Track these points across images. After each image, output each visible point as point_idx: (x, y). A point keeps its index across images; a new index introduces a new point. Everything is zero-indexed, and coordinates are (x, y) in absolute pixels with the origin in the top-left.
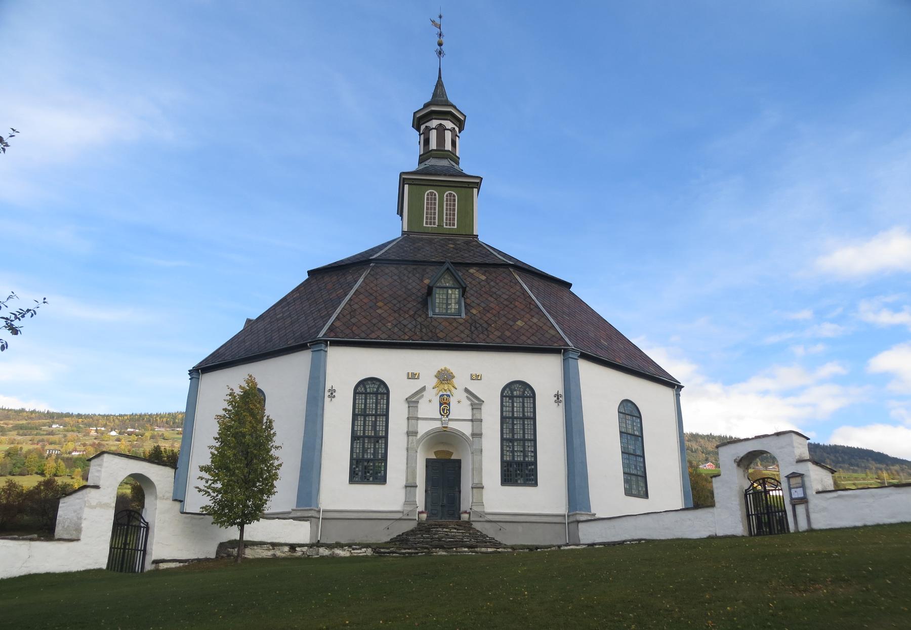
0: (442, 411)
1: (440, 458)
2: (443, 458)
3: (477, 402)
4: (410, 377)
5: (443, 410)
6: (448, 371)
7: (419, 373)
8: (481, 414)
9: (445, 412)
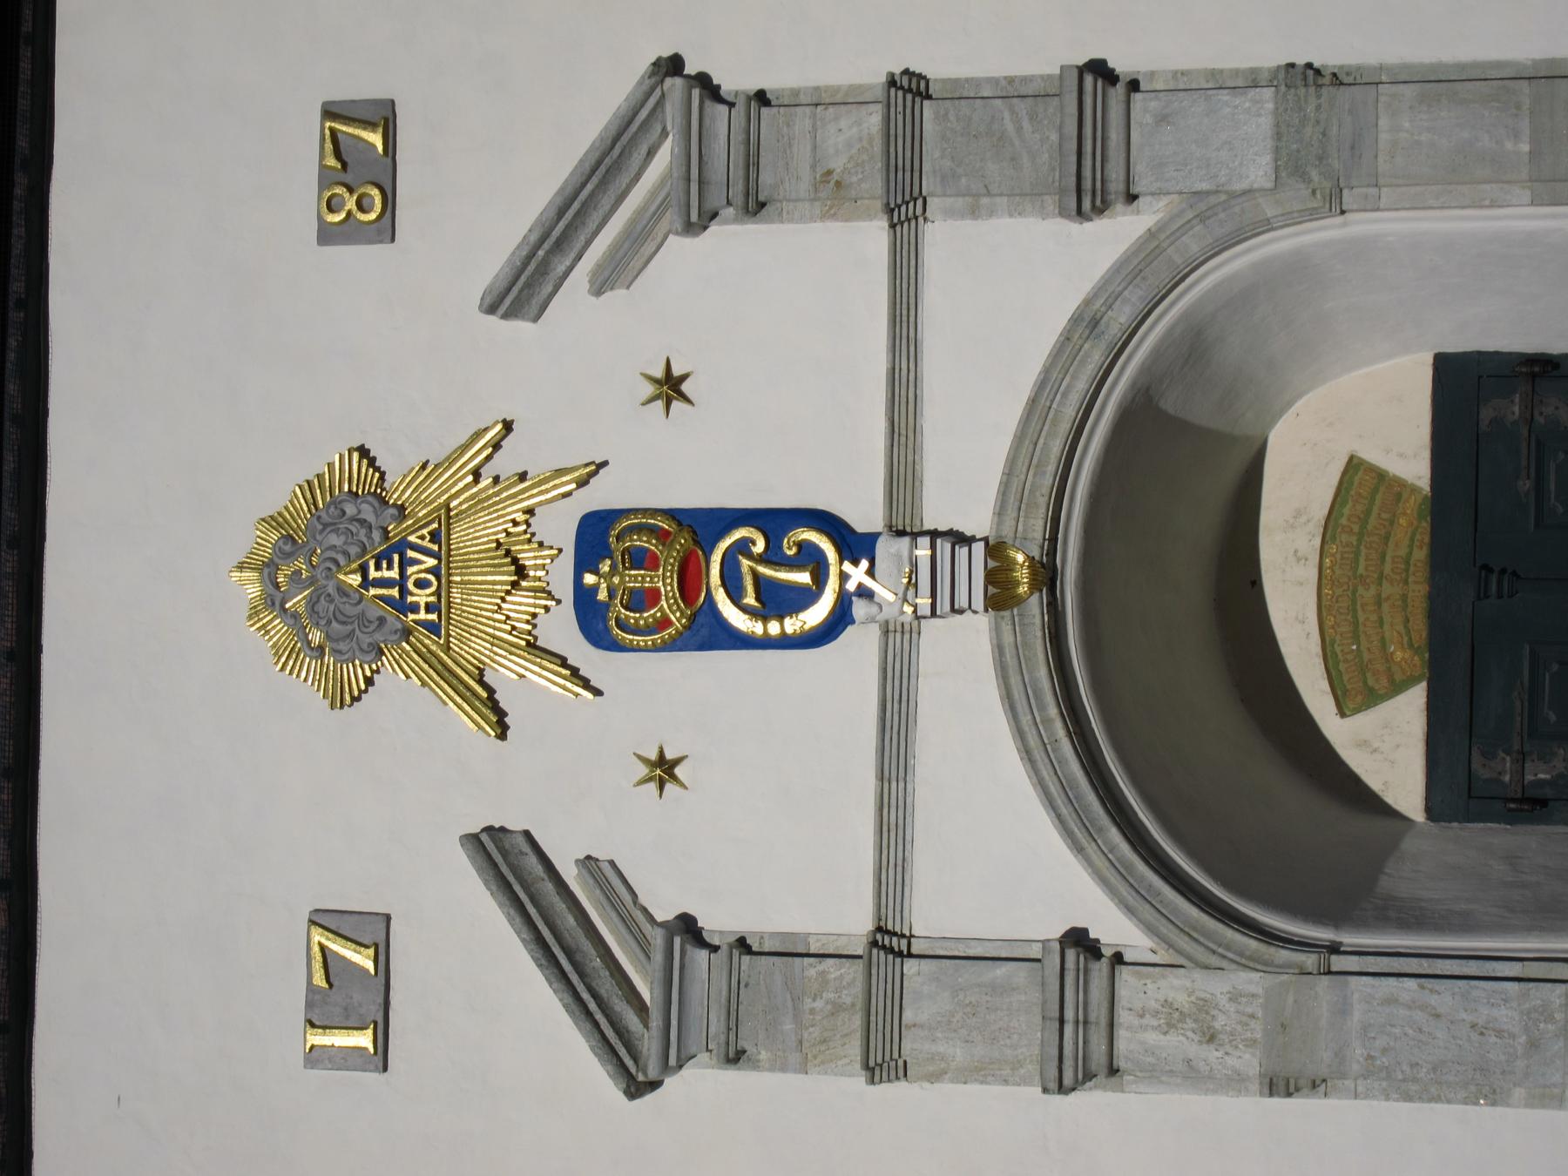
0: (792, 625)
1: (1420, 627)
2: (1418, 590)
3: (664, 157)
4: (364, 1040)
5: (777, 602)
6: (290, 545)
7: (319, 919)
8: (821, 101)
9: (804, 578)
